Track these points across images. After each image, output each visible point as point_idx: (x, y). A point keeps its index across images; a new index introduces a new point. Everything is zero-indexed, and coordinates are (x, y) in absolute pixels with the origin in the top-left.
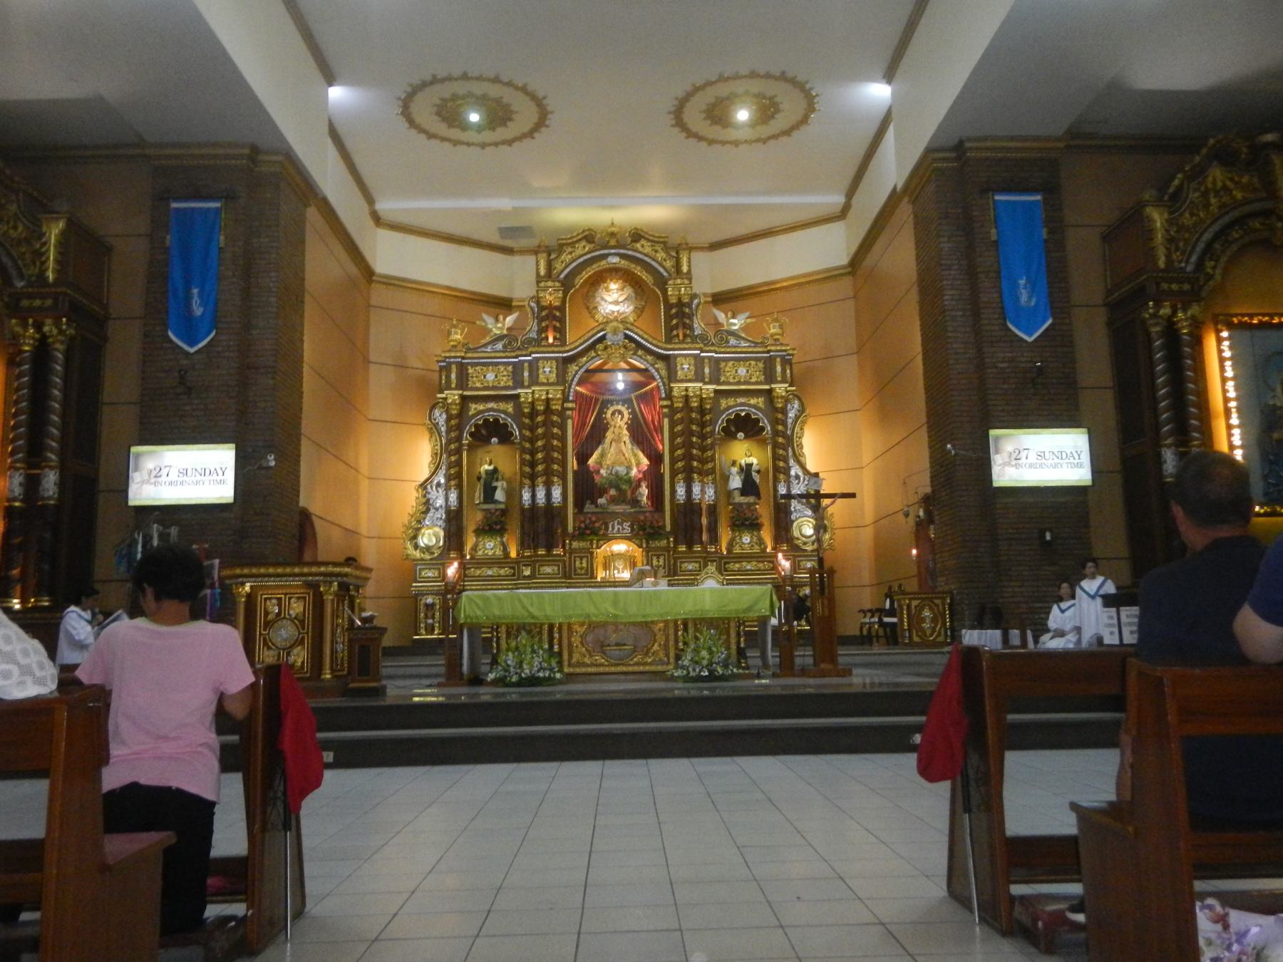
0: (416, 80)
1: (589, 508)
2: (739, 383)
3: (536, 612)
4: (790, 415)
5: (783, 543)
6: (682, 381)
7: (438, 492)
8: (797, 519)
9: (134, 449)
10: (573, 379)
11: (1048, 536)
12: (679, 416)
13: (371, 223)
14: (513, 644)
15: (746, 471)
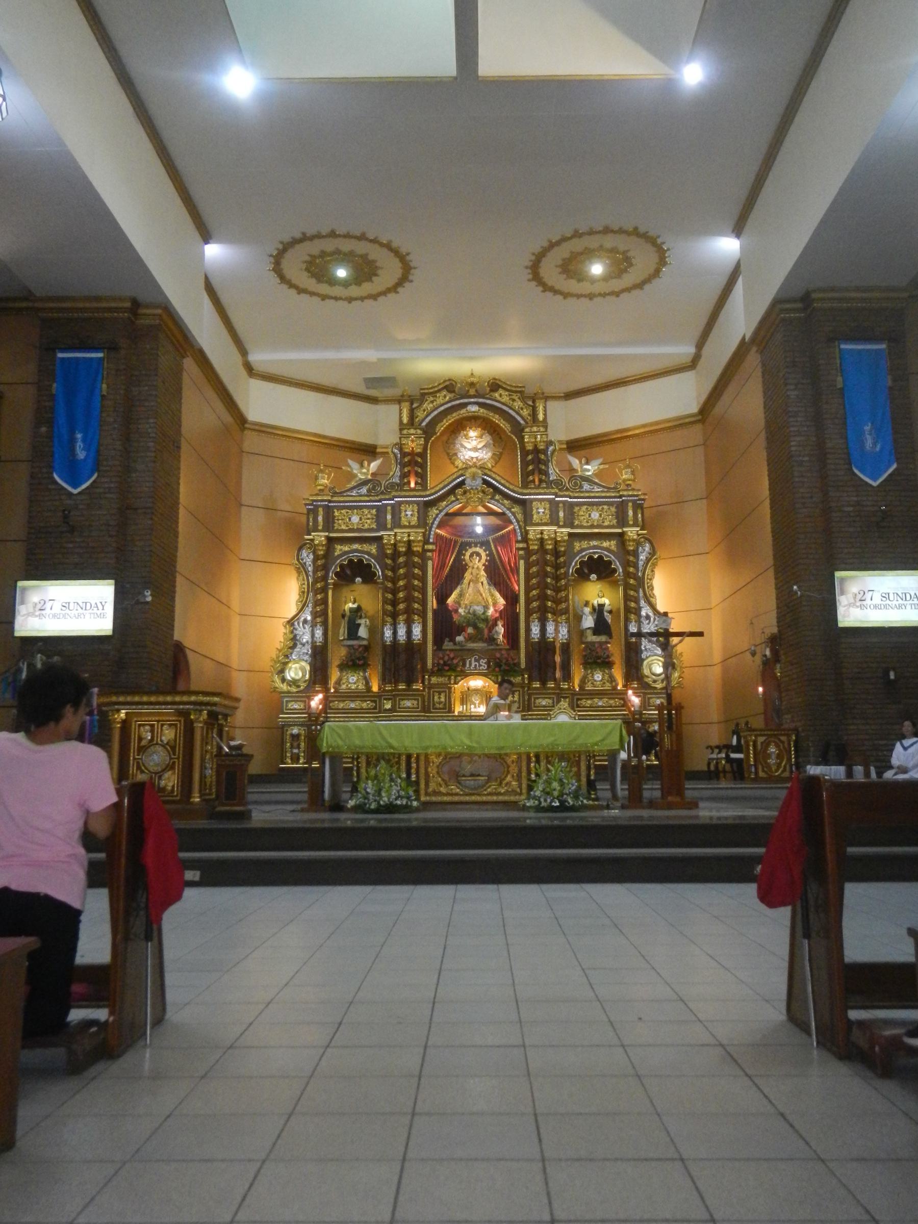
0: (287, 238)
1: (448, 645)
2: (592, 526)
4: (641, 557)
5: (632, 681)
7: (304, 628)
8: (647, 658)
9: (20, 584)
10: (433, 523)
11: (892, 676)
12: (534, 558)
13: (243, 372)
14: (373, 773)
15: (599, 611)
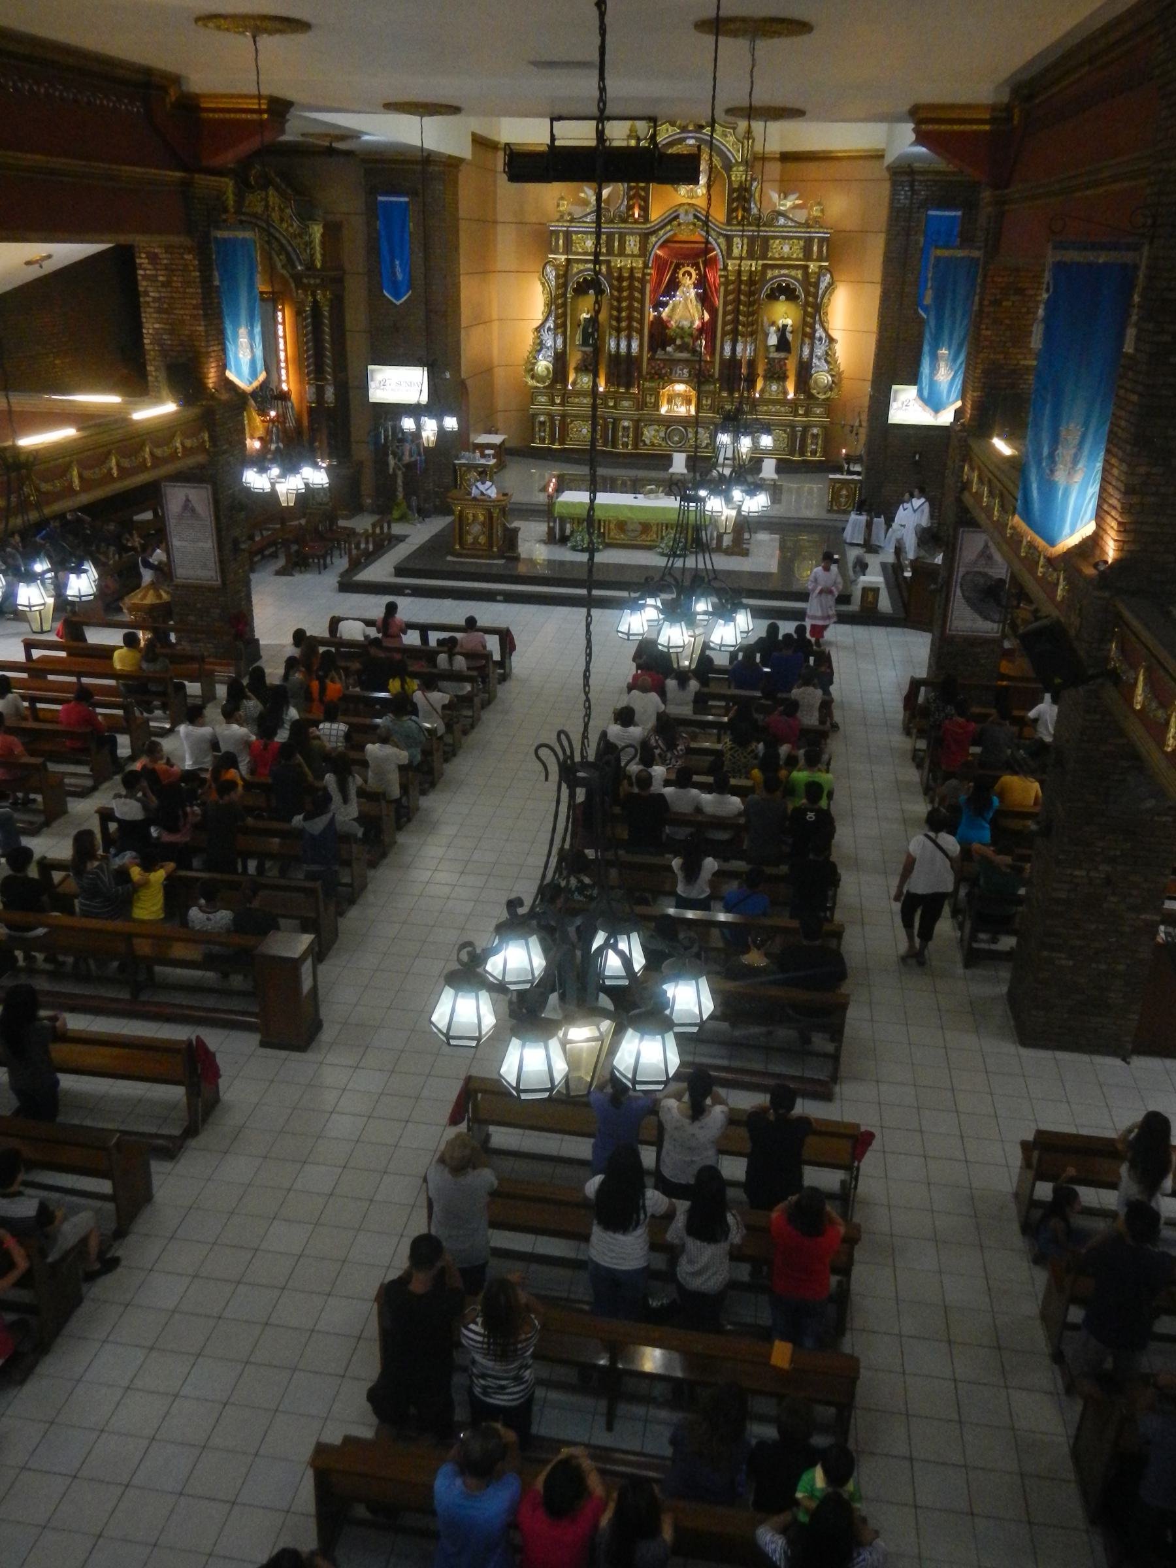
1: (660, 354)
9: (370, 367)
11: (917, 458)
12: (731, 287)
15: (782, 331)
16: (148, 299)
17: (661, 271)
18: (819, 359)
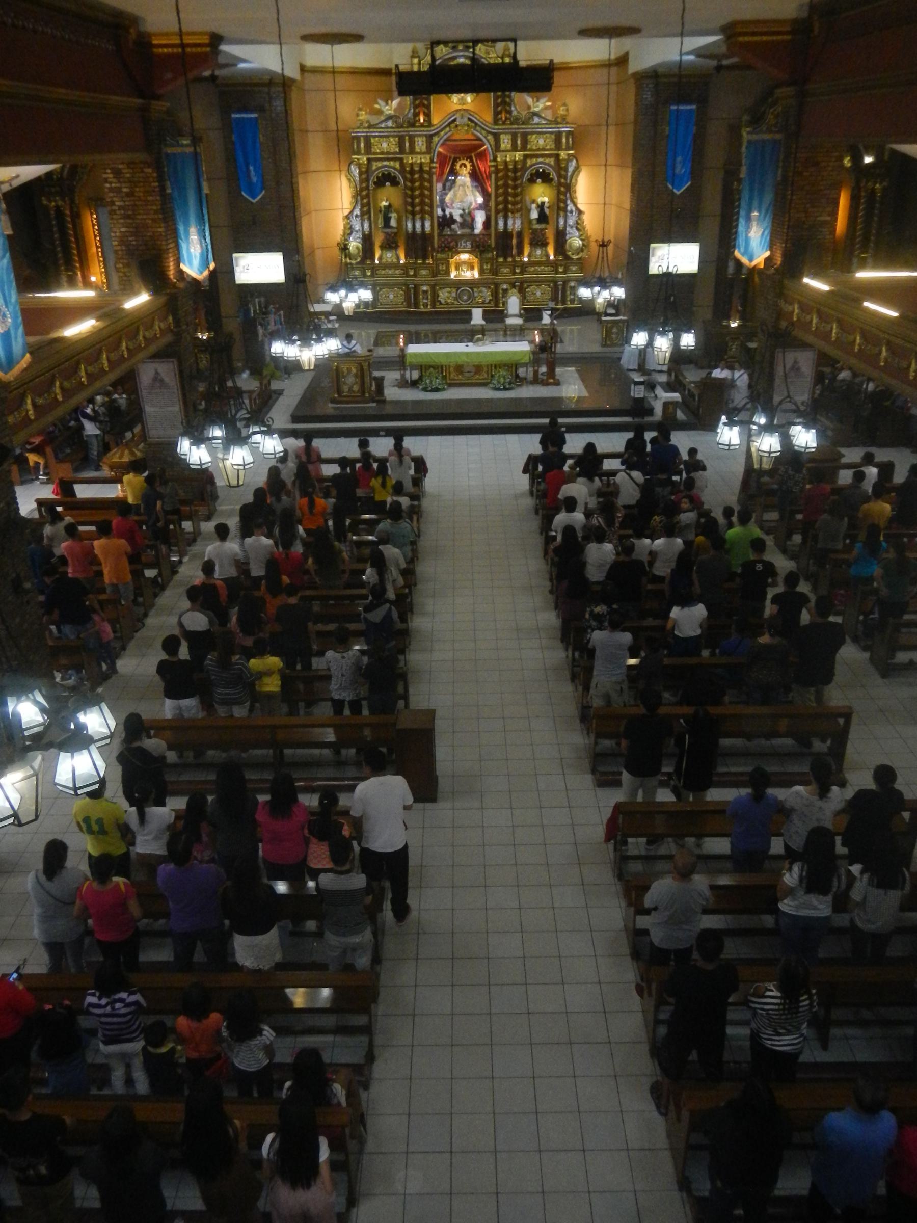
1: (447, 232)
3: (436, 361)
6: (503, 151)
9: (235, 255)
12: (501, 174)
15: (541, 207)
16: (114, 208)
17: (442, 164)
18: (571, 227)
